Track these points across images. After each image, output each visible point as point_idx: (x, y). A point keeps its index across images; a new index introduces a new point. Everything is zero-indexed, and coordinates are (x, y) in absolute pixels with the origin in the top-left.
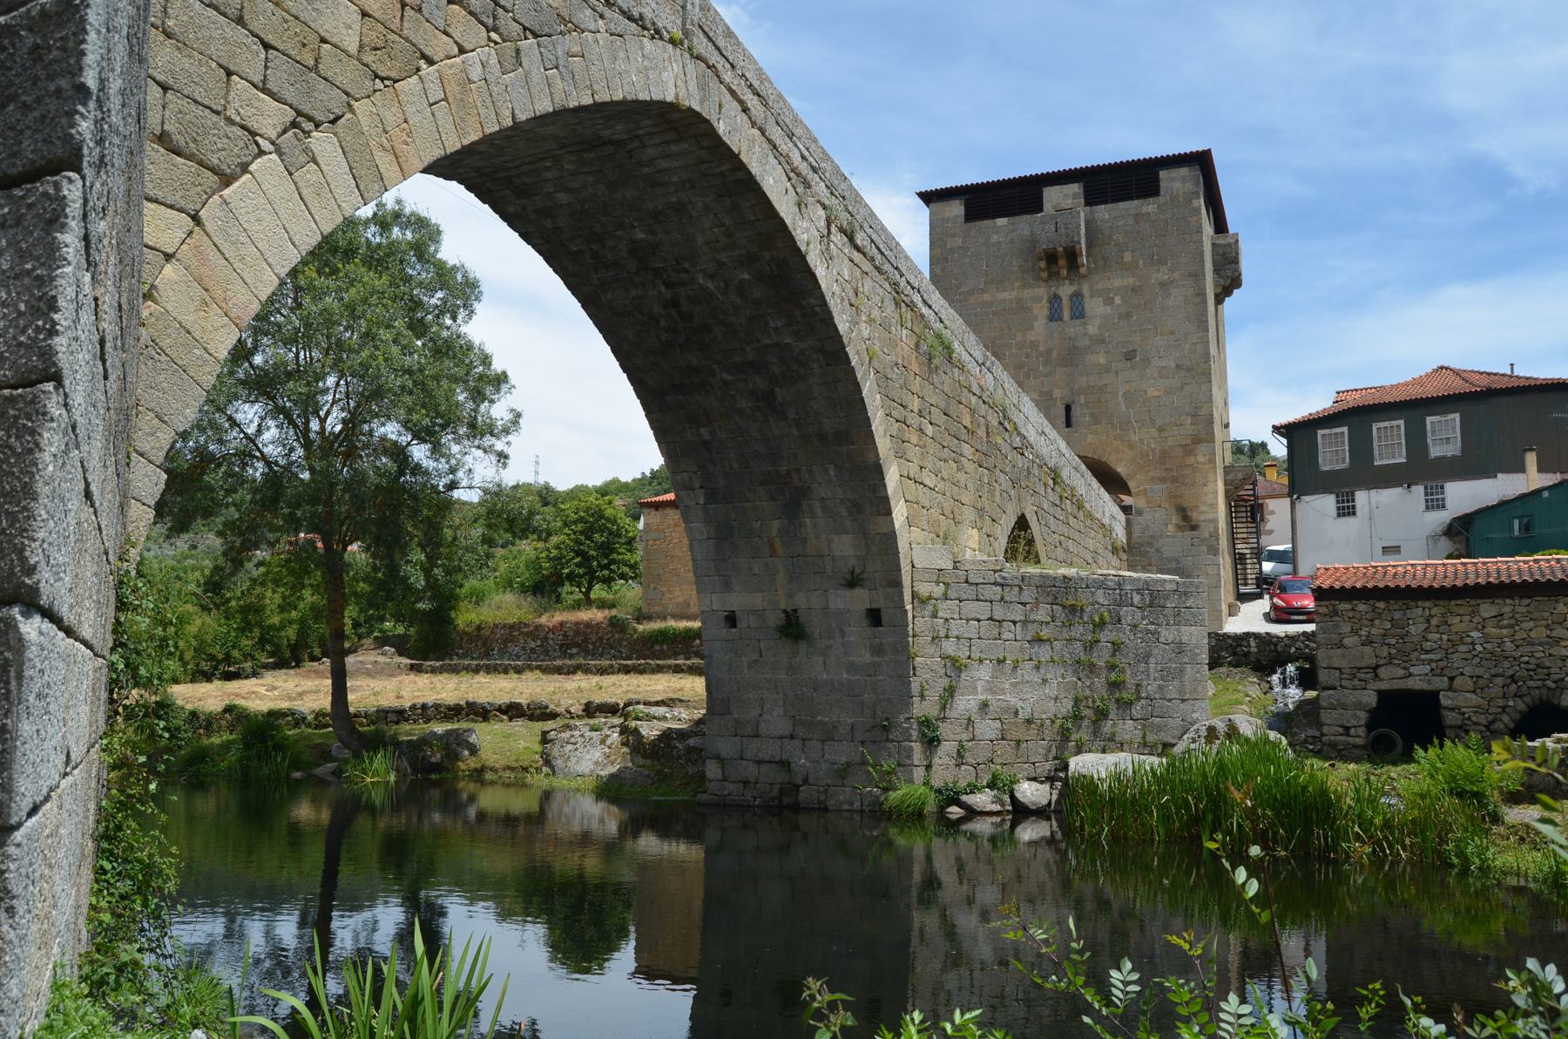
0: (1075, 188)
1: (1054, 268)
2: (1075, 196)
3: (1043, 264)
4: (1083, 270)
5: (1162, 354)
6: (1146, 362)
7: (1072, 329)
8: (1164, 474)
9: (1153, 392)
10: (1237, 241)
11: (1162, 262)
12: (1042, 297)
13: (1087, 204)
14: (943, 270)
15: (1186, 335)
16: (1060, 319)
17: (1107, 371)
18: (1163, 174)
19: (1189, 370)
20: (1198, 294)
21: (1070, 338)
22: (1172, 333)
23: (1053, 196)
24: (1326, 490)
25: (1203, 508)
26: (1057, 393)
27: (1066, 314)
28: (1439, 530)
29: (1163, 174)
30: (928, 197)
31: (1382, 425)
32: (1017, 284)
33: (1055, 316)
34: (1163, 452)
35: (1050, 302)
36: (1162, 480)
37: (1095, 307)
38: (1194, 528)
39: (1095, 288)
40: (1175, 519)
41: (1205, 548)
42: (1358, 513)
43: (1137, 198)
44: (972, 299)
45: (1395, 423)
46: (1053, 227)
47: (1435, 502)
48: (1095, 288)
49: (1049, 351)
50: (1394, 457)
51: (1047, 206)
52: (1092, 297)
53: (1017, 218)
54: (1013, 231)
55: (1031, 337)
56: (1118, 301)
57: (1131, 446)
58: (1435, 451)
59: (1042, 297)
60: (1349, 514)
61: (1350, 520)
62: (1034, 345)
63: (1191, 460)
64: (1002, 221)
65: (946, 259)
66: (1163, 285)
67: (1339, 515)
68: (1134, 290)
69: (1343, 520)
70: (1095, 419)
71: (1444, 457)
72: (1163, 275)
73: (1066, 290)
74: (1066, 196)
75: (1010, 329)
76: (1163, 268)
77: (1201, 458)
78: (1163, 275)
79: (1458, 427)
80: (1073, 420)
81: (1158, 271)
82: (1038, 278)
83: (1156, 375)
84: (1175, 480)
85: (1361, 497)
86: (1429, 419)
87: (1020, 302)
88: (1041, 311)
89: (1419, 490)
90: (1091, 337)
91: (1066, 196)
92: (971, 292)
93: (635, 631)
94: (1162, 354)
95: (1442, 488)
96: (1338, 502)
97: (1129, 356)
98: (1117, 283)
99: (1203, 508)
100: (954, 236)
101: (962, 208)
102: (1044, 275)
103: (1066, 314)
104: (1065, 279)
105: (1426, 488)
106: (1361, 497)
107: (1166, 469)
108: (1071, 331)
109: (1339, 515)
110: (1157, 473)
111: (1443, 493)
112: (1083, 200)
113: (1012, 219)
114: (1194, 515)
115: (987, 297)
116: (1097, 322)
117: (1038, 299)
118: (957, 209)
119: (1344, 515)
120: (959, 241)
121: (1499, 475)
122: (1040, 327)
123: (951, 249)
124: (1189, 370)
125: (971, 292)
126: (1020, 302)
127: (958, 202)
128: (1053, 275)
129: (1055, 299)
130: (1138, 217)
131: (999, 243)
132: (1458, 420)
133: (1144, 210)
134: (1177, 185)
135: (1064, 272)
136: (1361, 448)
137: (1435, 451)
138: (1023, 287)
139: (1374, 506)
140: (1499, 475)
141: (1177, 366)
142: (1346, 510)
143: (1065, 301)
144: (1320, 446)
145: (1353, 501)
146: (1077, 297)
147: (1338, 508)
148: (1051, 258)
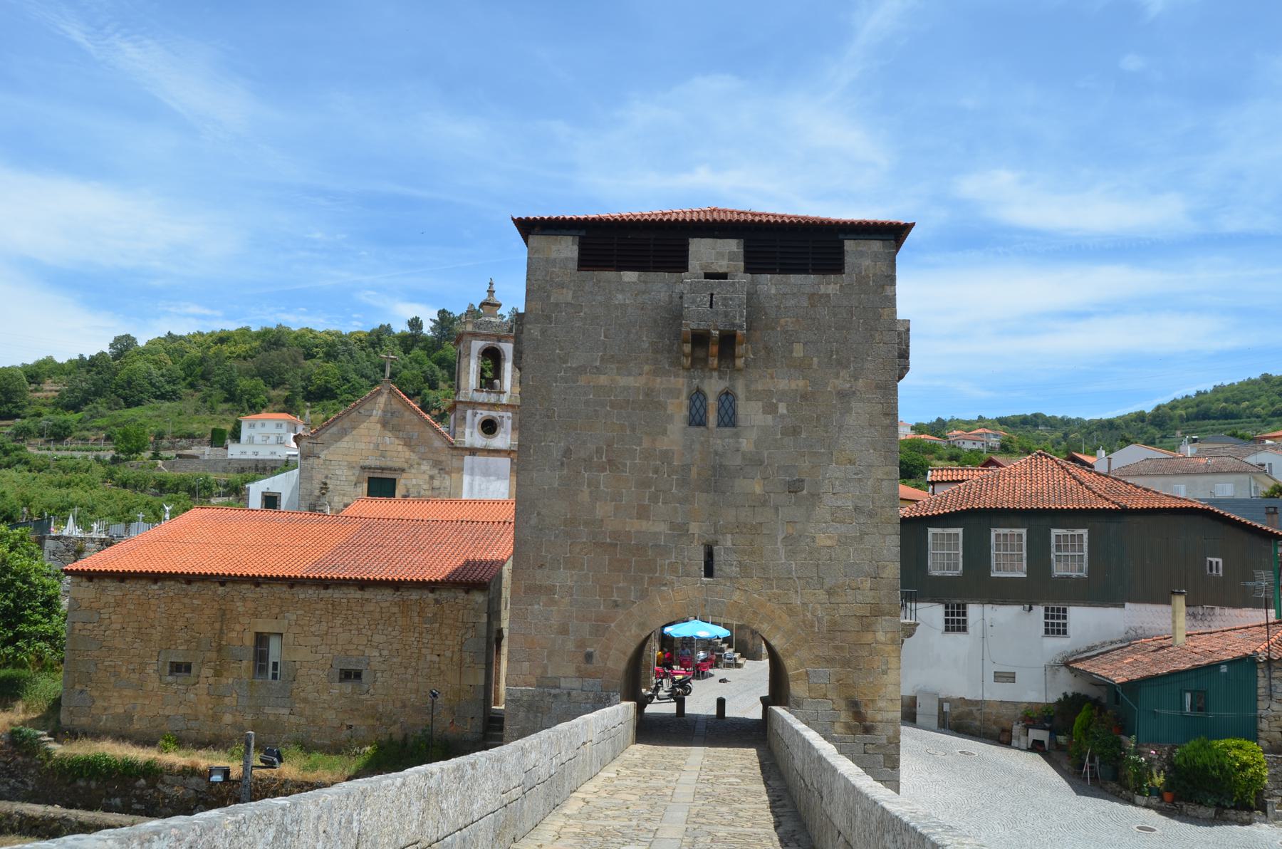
0: (732, 246)
1: (700, 353)
2: (732, 257)
3: (687, 348)
4: (740, 363)
5: (838, 489)
6: (815, 497)
7: (719, 439)
8: (832, 653)
9: (823, 540)
10: (908, 330)
11: (843, 364)
12: (679, 391)
13: (747, 270)
14: (543, 332)
17: (764, 504)
18: (849, 245)
19: (871, 515)
20: (886, 414)
21: (716, 453)
22: (851, 462)
23: (703, 252)
24: (934, 598)
25: (881, 704)
26: (694, 528)
27: (712, 418)
28: (1058, 659)
30: (527, 227)
31: (1002, 531)
32: (646, 368)
33: (696, 419)
34: (833, 623)
35: (690, 398)
36: (829, 661)
37: (750, 412)
38: (868, 730)
39: (753, 387)
40: (845, 716)
41: (881, 758)
42: (970, 629)
43: (816, 271)
44: (582, 380)
45: (1016, 531)
47: (1056, 627)
48: (753, 387)
49: (686, 468)
50: (1013, 570)
51: (694, 264)
52: (748, 399)
53: (652, 275)
54: (644, 292)
55: (663, 444)
56: (782, 409)
57: (791, 611)
58: (1058, 570)
59: (679, 391)
60: (959, 630)
61: (960, 636)
62: (666, 456)
63: (868, 638)
64: (630, 276)
65: (549, 318)
66: (843, 395)
67: (947, 629)
68: (804, 397)
69: (952, 635)
70: (745, 571)
71: (1068, 577)
72: (841, 382)
73: (714, 386)
74: (720, 255)
75: (633, 430)
77: (881, 636)
79: (1085, 544)
80: (716, 567)
81: (837, 376)
82: (676, 363)
83: (828, 517)
84: (846, 663)
85: (974, 612)
86: (1055, 532)
87: (649, 393)
88: (678, 409)
89: (1039, 611)
90: (744, 454)
91: (720, 255)
92: (582, 370)
93: (49, 754)
94: (838, 489)
95: (1065, 611)
96: (947, 614)
97: (794, 487)
98: (783, 384)
99: (881, 704)
100: (561, 286)
101: (576, 248)
102: (687, 362)
103: (712, 418)
104: (715, 369)
105: (1047, 610)
106: (974, 612)
107: (836, 648)
108: (718, 444)
109: (947, 629)
111: (1065, 618)
112: (742, 264)
114: (870, 713)
115: (603, 380)
117: (674, 393)
118: (567, 249)
119: (953, 630)
120: (567, 295)
121: (1127, 605)
122: (675, 434)
123: (557, 305)
124: (871, 515)
125: (582, 370)
126: (649, 393)
127: (570, 238)
128: (698, 362)
129: (697, 396)
130: (815, 298)
131: (623, 306)
132: (1086, 537)
133: (823, 290)
134: (867, 262)
135: (714, 362)
136: (977, 553)
137: (1058, 570)
138: (656, 372)
139: (988, 622)
140: (1127, 605)
141: (856, 508)
142: (956, 624)
143: (712, 402)
144: (930, 546)
145: (964, 614)
146: (728, 397)
147: (947, 621)
148: (700, 339)
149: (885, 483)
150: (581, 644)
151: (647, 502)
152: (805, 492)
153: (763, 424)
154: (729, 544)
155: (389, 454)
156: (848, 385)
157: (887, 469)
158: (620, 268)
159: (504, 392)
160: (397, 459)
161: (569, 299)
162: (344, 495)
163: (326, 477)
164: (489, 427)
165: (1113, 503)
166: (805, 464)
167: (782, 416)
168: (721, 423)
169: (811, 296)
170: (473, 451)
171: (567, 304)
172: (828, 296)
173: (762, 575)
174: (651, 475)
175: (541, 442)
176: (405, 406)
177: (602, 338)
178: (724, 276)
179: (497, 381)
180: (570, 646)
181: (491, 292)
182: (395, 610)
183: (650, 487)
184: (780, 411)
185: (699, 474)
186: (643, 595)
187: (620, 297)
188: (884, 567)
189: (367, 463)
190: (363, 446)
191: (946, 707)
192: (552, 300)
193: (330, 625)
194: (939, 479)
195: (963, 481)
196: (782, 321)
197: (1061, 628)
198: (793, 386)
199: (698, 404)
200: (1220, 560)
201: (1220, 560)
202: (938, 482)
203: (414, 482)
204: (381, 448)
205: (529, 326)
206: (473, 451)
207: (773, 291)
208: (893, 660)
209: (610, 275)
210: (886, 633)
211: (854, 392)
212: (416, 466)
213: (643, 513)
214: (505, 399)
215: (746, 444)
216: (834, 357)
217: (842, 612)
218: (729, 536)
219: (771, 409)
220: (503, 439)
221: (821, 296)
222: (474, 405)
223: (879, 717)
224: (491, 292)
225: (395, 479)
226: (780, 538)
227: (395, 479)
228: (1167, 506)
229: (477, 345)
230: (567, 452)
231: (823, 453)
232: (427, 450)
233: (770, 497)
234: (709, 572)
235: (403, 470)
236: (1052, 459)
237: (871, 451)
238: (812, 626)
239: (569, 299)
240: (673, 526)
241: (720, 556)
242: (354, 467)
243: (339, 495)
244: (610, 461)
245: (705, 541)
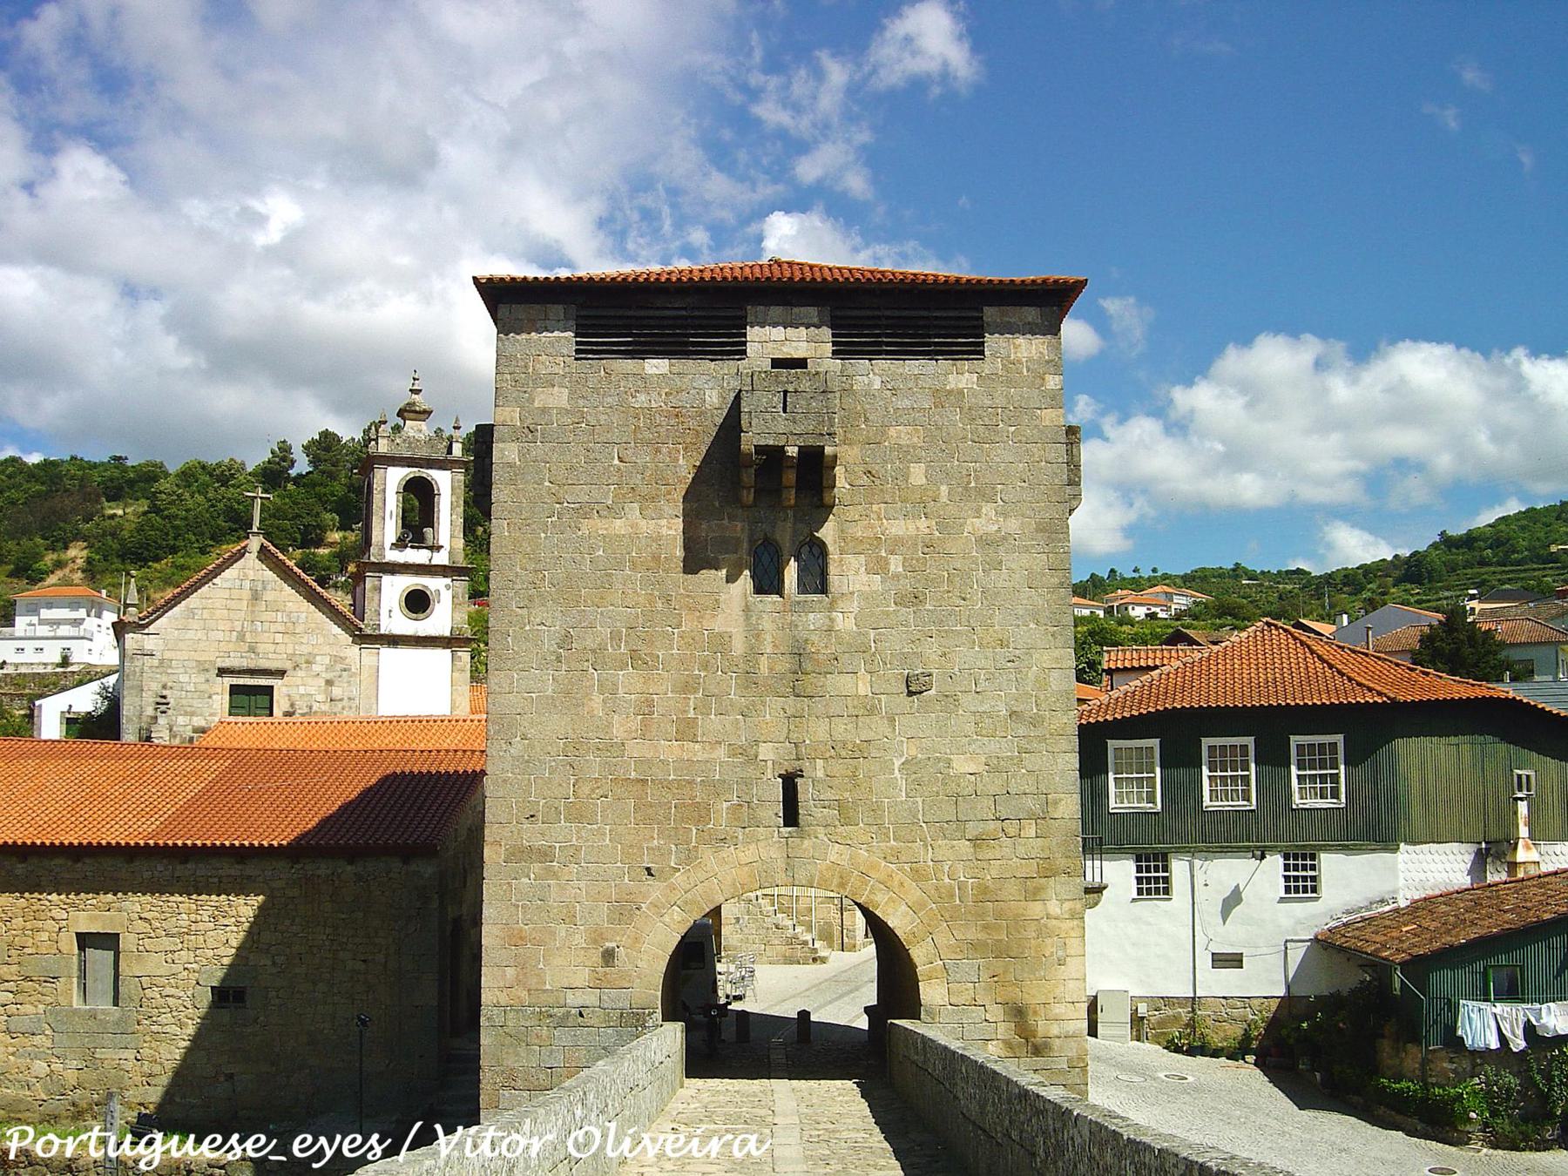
8: (982, 936)
9: (962, 765)
14: (522, 455)
15: (1030, 649)
16: (779, 590)
17: (872, 711)
19: (1035, 722)
25: (1059, 1009)
26: (766, 752)
29: (990, 313)
34: (984, 890)
37: (847, 572)
40: (1005, 1030)
46: (778, 399)
47: (1302, 884)
53: (688, 365)
56: (896, 564)
59: (738, 541)
60: (1157, 891)
62: (720, 642)
63: (1036, 909)
64: (656, 366)
66: (985, 542)
72: (986, 521)
76: (988, 509)
77: (1054, 907)
78: (986, 521)
83: (970, 728)
84: (1001, 951)
89: (1275, 862)
92: (583, 511)
95: (1313, 857)
96: (1139, 869)
102: (748, 497)
106: (1179, 868)
110: (973, 934)
112: (829, 348)
113: (681, 365)
115: (619, 526)
116: (854, 606)
119: (1149, 891)
124: (1035, 722)
130: (942, 397)
135: (791, 497)
141: (1013, 714)
142: (1154, 885)
145: (1165, 869)
149: (1055, 674)
150: (597, 937)
151: (691, 714)
152: (933, 692)
153: (867, 588)
154: (820, 774)
155: (261, 648)
156: (995, 528)
157: (1057, 653)
158: (639, 352)
159: (439, 548)
160: (275, 656)
161: (564, 403)
162: (192, 714)
163: (164, 687)
164: (418, 603)
165: (1380, 694)
166: (931, 650)
167: (896, 576)
168: (803, 588)
169: (935, 392)
170: (394, 641)
171: (561, 411)
172: (961, 392)
173: (871, 821)
174: (697, 672)
175: (525, 625)
176: (285, 572)
177: (616, 462)
178: (801, 363)
179: (428, 530)
180: (579, 939)
182: (295, 892)
183: (696, 691)
184: (892, 568)
185: (771, 669)
186: (690, 858)
187: (642, 397)
188: (1056, 803)
189: (227, 663)
190: (220, 636)
191: (1142, 1009)
192: (536, 405)
193: (193, 917)
194: (1120, 666)
195: (1156, 667)
196: (892, 432)
197: (1309, 884)
198: (912, 531)
199: (766, 559)
200: (1531, 773)
201: (1531, 773)
202: (1118, 669)
203: (302, 690)
204: (248, 638)
205: (501, 445)
206: (394, 641)
207: (877, 385)
208: (1073, 944)
209: (629, 365)
210: (1062, 901)
211: (1004, 538)
212: (304, 666)
213: (686, 731)
214: (441, 558)
215: (845, 623)
216: (973, 484)
217: (994, 874)
218: (820, 763)
219: (878, 567)
220: (440, 621)
221: (950, 392)
223: (1055, 1030)
225: (272, 687)
226: (897, 763)
227: (272, 687)
228: (1457, 697)
229: (393, 479)
230: (566, 640)
231: (959, 632)
232: (321, 640)
233: (880, 700)
234: (791, 815)
235: (281, 673)
236: (1285, 630)
237: (1032, 626)
238: (952, 896)
239: (564, 403)
240: (734, 751)
242: (207, 670)
243: (186, 714)
244: (634, 654)
245: (784, 772)
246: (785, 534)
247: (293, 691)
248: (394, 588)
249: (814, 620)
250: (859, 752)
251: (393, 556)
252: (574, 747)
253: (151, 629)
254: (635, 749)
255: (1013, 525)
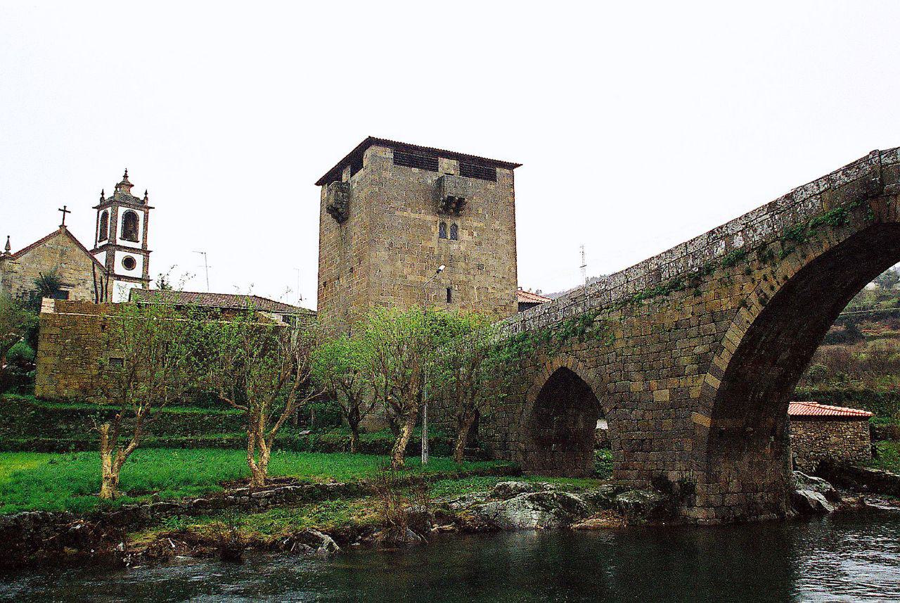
0: (454, 162)
37: (464, 235)
55: (430, 245)
72: (497, 225)
73: (449, 222)
76: (497, 222)
88: (436, 230)
118: (389, 154)
129: (443, 224)
170: (119, 278)
181: (126, 176)
206: (119, 278)
219: (471, 234)
222: (120, 248)
224: (126, 176)
234: (449, 300)
235: (73, 286)
241: (453, 294)
246: (449, 222)
247: (77, 295)
248: (120, 256)
249: (454, 246)
250: (466, 283)
251: (119, 242)
252: (393, 275)
253: (17, 261)
254: (410, 278)
255: (503, 228)
